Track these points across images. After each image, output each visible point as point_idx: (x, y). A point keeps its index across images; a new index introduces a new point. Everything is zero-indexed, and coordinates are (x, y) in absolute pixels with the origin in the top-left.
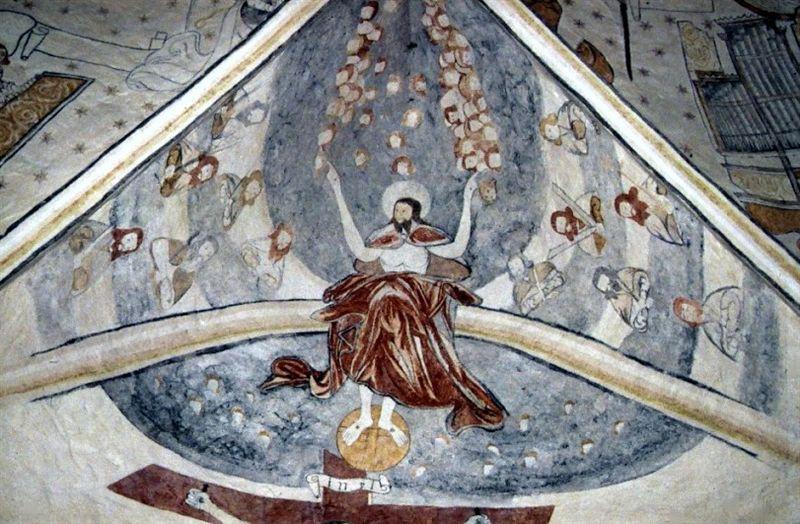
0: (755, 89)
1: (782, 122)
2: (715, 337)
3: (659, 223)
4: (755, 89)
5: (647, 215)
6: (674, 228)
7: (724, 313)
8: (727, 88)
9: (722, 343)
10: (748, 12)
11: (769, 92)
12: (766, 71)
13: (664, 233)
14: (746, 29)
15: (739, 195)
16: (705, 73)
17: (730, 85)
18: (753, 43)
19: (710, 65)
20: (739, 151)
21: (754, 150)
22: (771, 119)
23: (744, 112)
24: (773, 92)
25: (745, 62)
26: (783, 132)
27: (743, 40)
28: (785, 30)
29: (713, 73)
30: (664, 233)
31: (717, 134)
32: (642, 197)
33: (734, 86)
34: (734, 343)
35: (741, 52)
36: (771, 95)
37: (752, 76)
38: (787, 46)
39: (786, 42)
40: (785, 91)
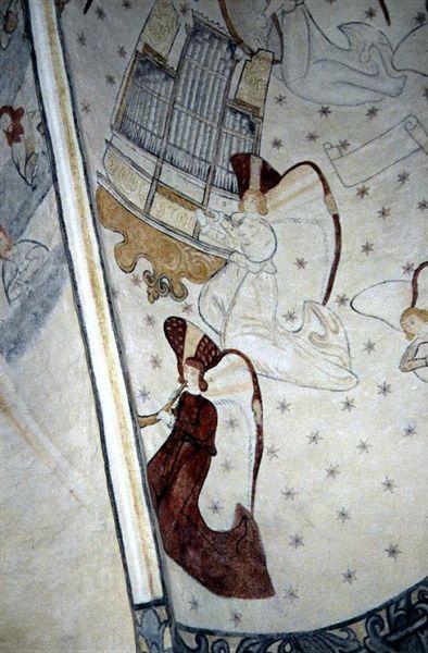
0: (180, 94)
1: (180, 137)
2: (8, 276)
3: (23, 155)
4: (180, 94)
5: (19, 140)
6: (33, 166)
7: (26, 262)
8: (159, 76)
9: (9, 284)
10: (223, 24)
11: (189, 104)
12: (200, 84)
13: (22, 164)
14: (210, 37)
15: (99, 175)
16: (152, 51)
17: (163, 76)
18: (208, 52)
19: (160, 48)
20: (128, 138)
21: (141, 146)
22: (174, 128)
23: (157, 107)
24: (192, 106)
25: (190, 64)
26: (174, 146)
27: (202, 44)
28: (238, 61)
29: (158, 55)
30: (22, 164)
31: (122, 110)
32: (24, 121)
33: (166, 79)
34: (18, 291)
35: (193, 53)
36: (188, 108)
37: (186, 80)
38: (231, 75)
39: (232, 71)
40: (202, 111)
